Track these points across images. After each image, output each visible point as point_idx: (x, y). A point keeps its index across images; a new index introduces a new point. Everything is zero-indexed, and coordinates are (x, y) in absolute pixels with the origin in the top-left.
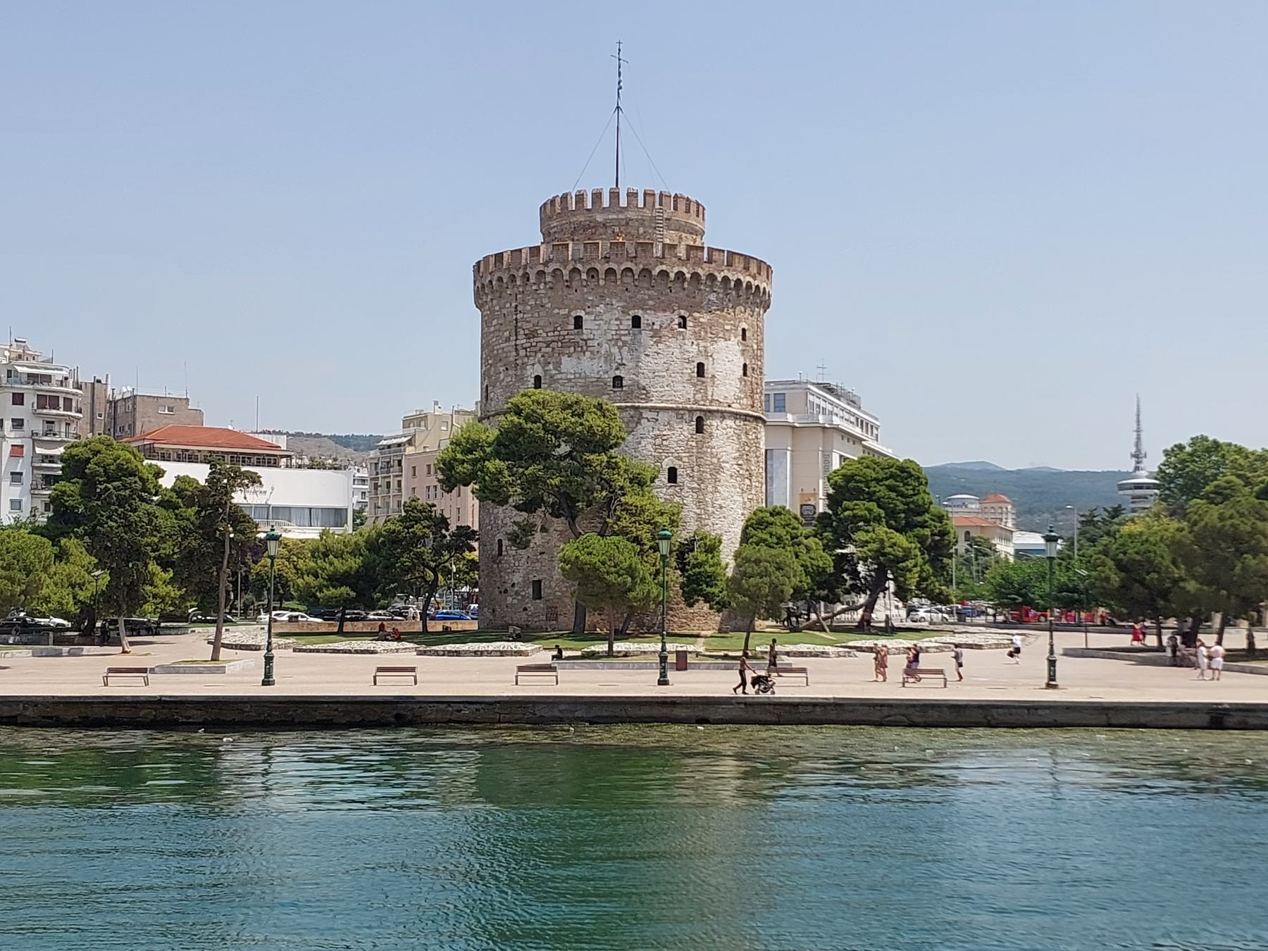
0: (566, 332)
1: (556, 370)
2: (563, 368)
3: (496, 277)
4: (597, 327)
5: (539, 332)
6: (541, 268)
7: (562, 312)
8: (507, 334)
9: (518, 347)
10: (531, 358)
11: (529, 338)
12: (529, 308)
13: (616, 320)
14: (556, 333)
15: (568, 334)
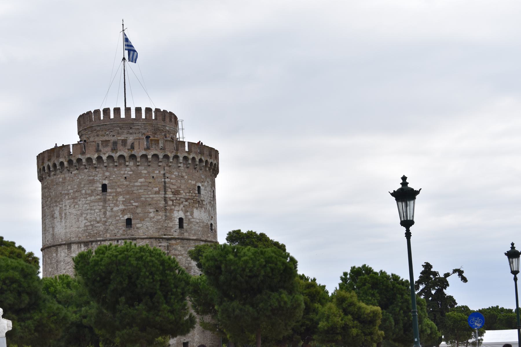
0: (195, 195)
1: (191, 216)
2: (195, 217)
3: (152, 153)
4: (205, 194)
5: (182, 192)
6: (186, 155)
7: (193, 182)
8: (157, 189)
9: (167, 199)
10: (177, 207)
11: (175, 194)
12: (174, 176)
13: (210, 191)
14: (190, 194)
15: (195, 196)
